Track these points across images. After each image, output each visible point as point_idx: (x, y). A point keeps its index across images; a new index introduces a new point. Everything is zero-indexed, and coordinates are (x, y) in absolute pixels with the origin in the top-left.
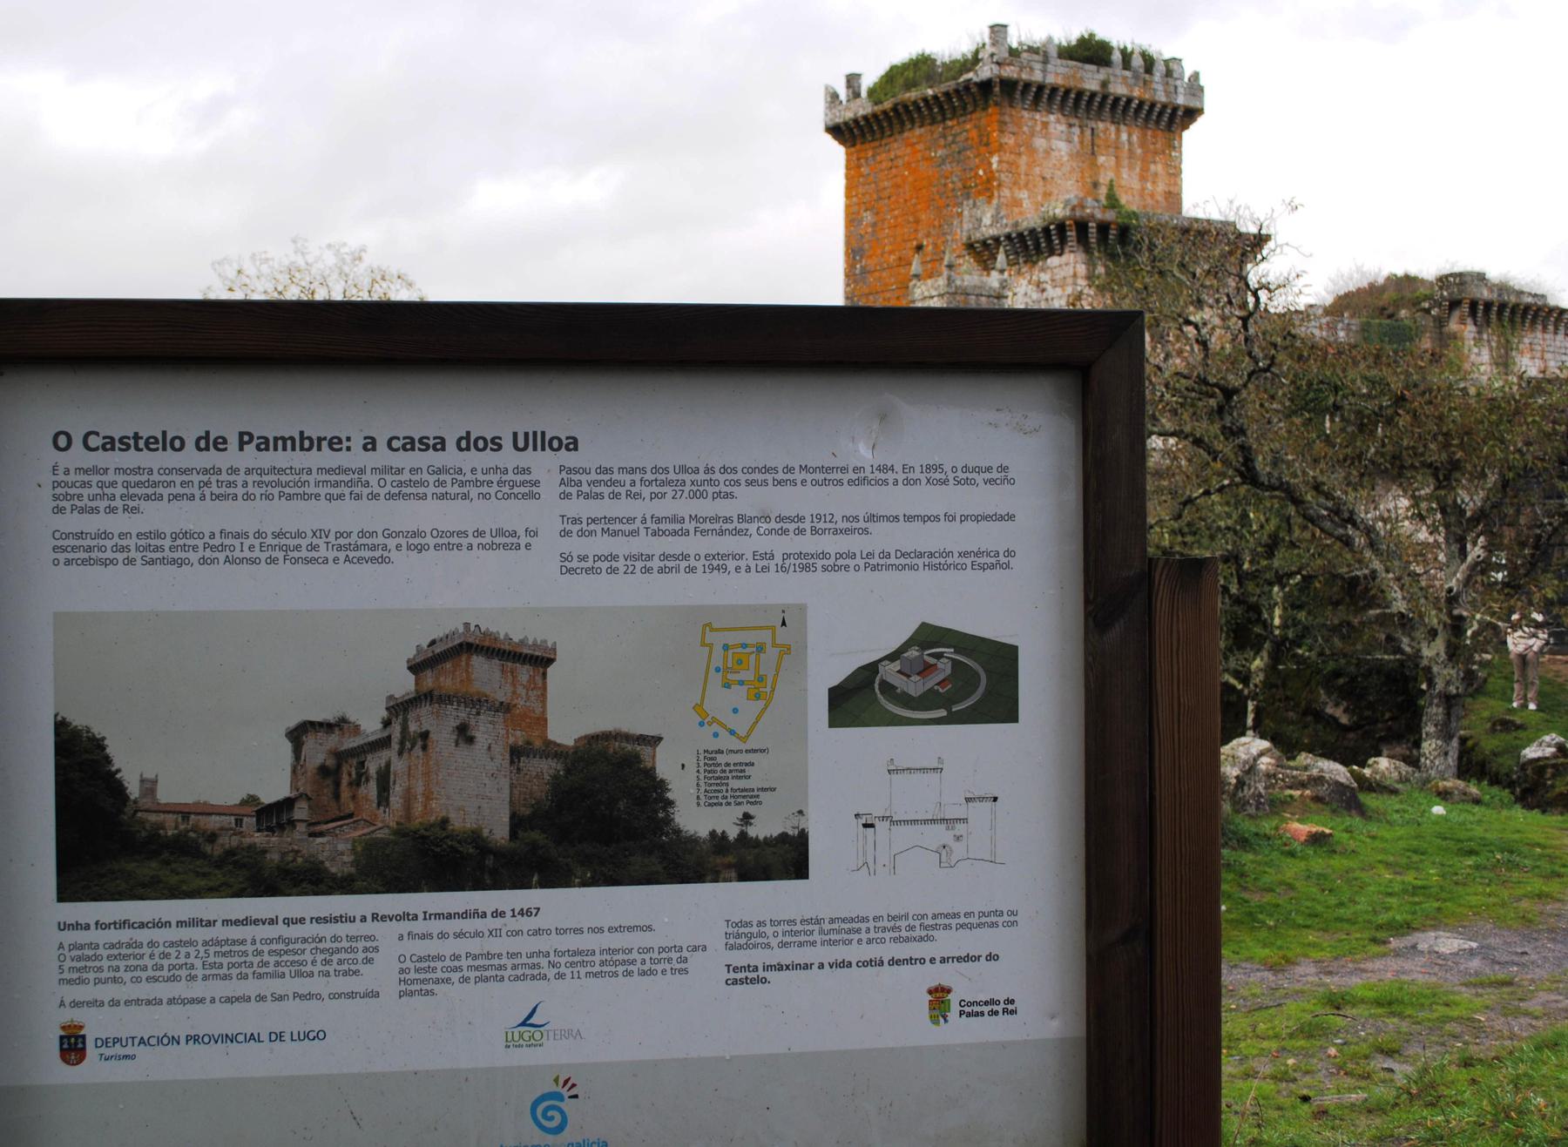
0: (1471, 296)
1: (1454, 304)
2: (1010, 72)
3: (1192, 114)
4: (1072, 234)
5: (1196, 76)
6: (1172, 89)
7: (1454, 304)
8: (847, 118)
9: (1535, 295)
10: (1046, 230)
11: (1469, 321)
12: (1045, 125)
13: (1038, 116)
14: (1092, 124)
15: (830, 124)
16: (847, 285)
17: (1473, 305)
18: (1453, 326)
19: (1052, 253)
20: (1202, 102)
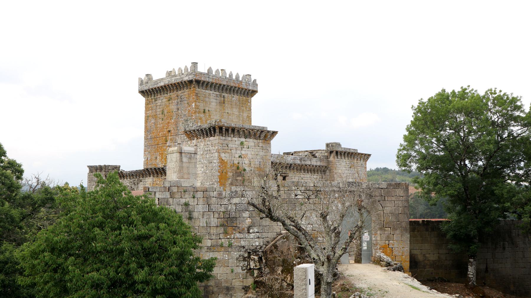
0: (336, 150)
1: (331, 152)
2: (198, 78)
3: (254, 92)
4: (217, 130)
5: (255, 80)
6: (248, 84)
7: (331, 152)
8: (146, 89)
10: (209, 129)
11: (336, 157)
12: (210, 94)
13: (207, 91)
14: (223, 94)
15: (141, 90)
16: (145, 142)
17: (337, 152)
18: (331, 159)
19: (211, 136)
20: (257, 89)
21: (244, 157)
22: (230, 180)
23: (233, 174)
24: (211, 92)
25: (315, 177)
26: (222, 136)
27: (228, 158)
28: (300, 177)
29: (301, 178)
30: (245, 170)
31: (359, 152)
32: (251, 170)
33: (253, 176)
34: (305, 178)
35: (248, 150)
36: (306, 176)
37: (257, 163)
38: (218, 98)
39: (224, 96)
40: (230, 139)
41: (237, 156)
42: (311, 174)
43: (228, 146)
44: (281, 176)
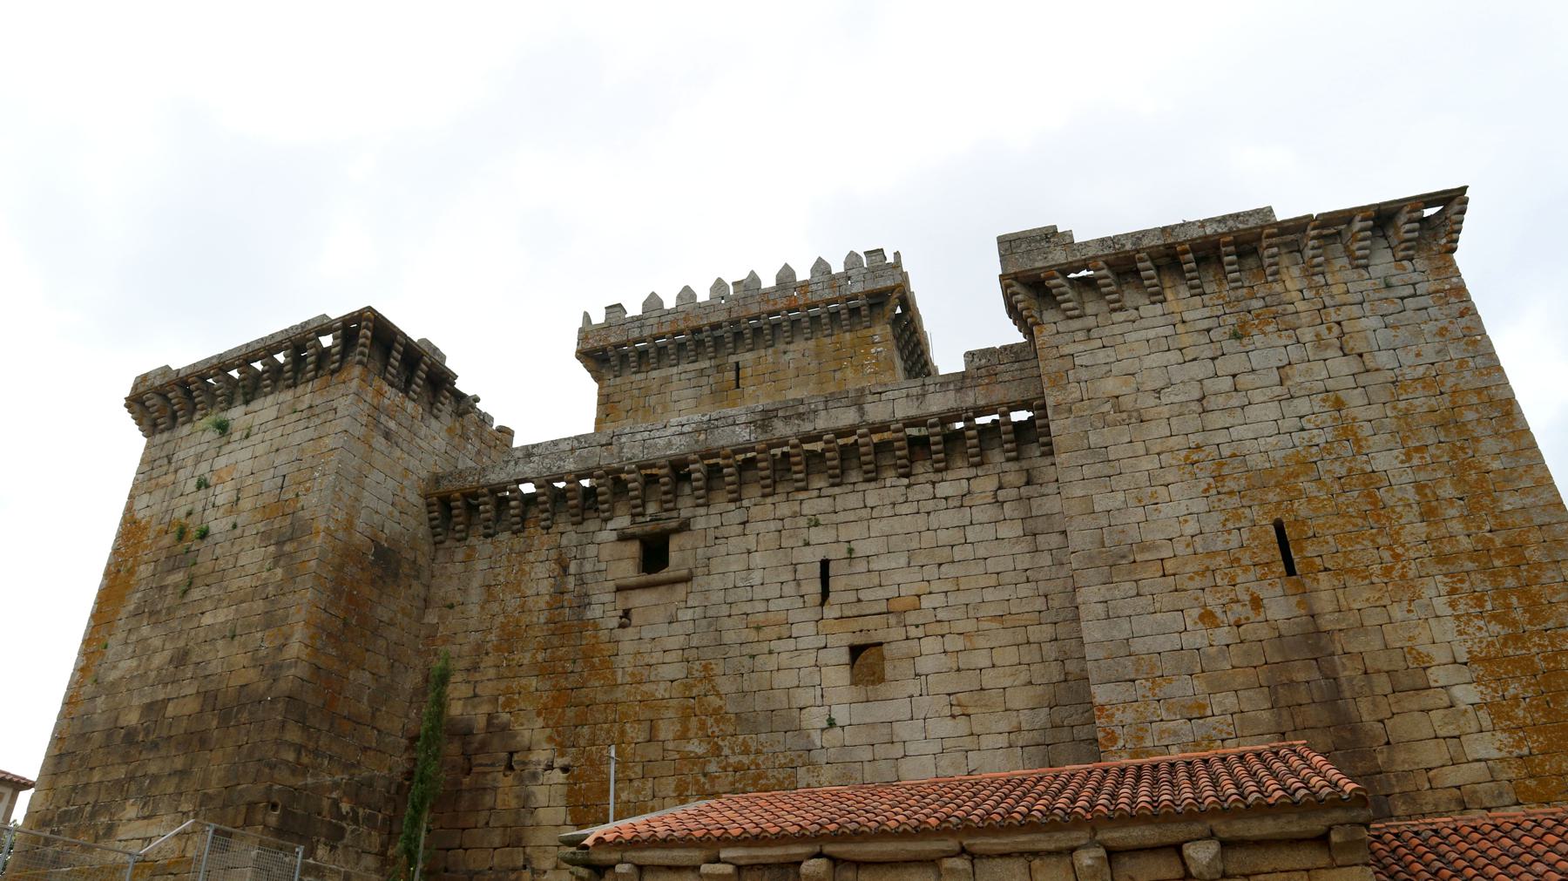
5: (897, 254)
9: (1222, 220)
12: (667, 381)
21: (220, 477)
22: (139, 595)
23: (155, 568)
24: (675, 370)
25: (944, 489)
26: (162, 431)
27: (156, 508)
28: (794, 516)
29: (803, 522)
30: (204, 535)
31: (1281, 215)
32: (235, 526)
33: (236, 549)
34: (841, 517)
35: (246, 443)
36: (853, 500)
37: (267, 486)
38: (704, 380)
39: (737, 363)
40: (186, 429)
41: (192, 484)
42: (905, 481)
43: (170, 462)
44: (624, 537)
